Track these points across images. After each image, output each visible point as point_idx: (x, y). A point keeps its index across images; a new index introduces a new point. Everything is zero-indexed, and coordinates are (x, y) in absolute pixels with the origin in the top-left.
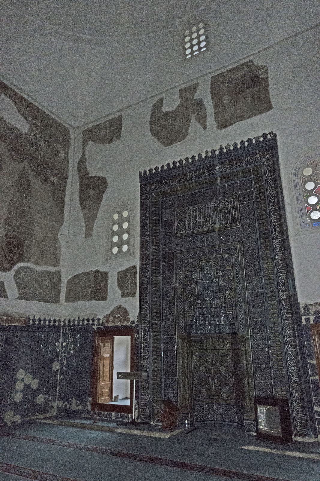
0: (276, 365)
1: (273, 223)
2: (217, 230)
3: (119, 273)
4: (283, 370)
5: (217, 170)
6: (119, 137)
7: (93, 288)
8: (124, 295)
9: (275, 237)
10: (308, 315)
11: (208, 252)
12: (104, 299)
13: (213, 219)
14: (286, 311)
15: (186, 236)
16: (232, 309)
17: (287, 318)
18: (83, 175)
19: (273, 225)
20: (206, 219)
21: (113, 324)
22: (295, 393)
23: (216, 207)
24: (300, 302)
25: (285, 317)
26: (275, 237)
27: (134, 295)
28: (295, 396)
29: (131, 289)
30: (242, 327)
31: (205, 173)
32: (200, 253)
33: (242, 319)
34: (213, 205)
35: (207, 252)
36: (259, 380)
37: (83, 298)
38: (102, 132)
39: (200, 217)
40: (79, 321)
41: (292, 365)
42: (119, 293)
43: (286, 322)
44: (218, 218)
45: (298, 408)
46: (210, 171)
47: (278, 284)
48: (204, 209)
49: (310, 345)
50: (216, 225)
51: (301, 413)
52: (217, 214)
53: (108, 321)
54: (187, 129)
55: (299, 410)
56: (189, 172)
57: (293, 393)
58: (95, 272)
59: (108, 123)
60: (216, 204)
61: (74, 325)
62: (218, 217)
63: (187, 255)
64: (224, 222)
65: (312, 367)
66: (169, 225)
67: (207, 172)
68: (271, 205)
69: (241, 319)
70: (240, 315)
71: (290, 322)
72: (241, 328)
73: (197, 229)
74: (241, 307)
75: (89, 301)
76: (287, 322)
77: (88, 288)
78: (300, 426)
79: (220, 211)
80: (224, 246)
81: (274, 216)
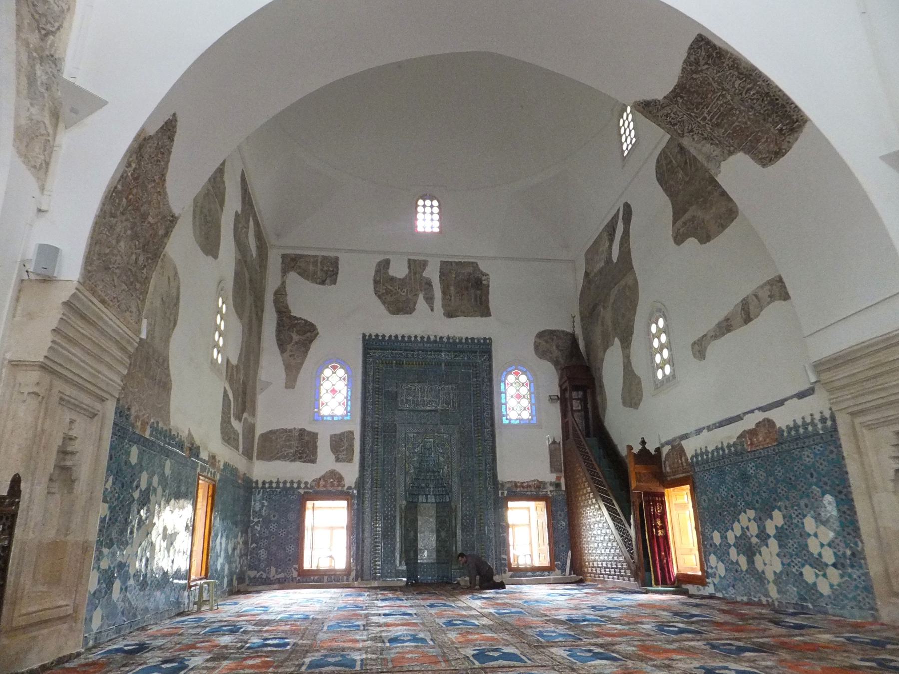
3: (331, 436)
6: (334, 282)
7: (297, 447)
8: (337, 460)
12: (313, 461)
15: (409, 411)
18: (283, 311)
20: (430, 398)
21: (324, 489)
27: (350, 460)
29: (346, 454)
37: (284, 458)
38: (311, 268)
40: (278, 482)
42: (333, 457)
47: (486, 465)
53: (318, 485)
54: (415, 303)
58: (301, 430)
59: (319, 260)
61: (270, 487)
66: (393, 397)
75: (291, 461)
77: (290, 447)
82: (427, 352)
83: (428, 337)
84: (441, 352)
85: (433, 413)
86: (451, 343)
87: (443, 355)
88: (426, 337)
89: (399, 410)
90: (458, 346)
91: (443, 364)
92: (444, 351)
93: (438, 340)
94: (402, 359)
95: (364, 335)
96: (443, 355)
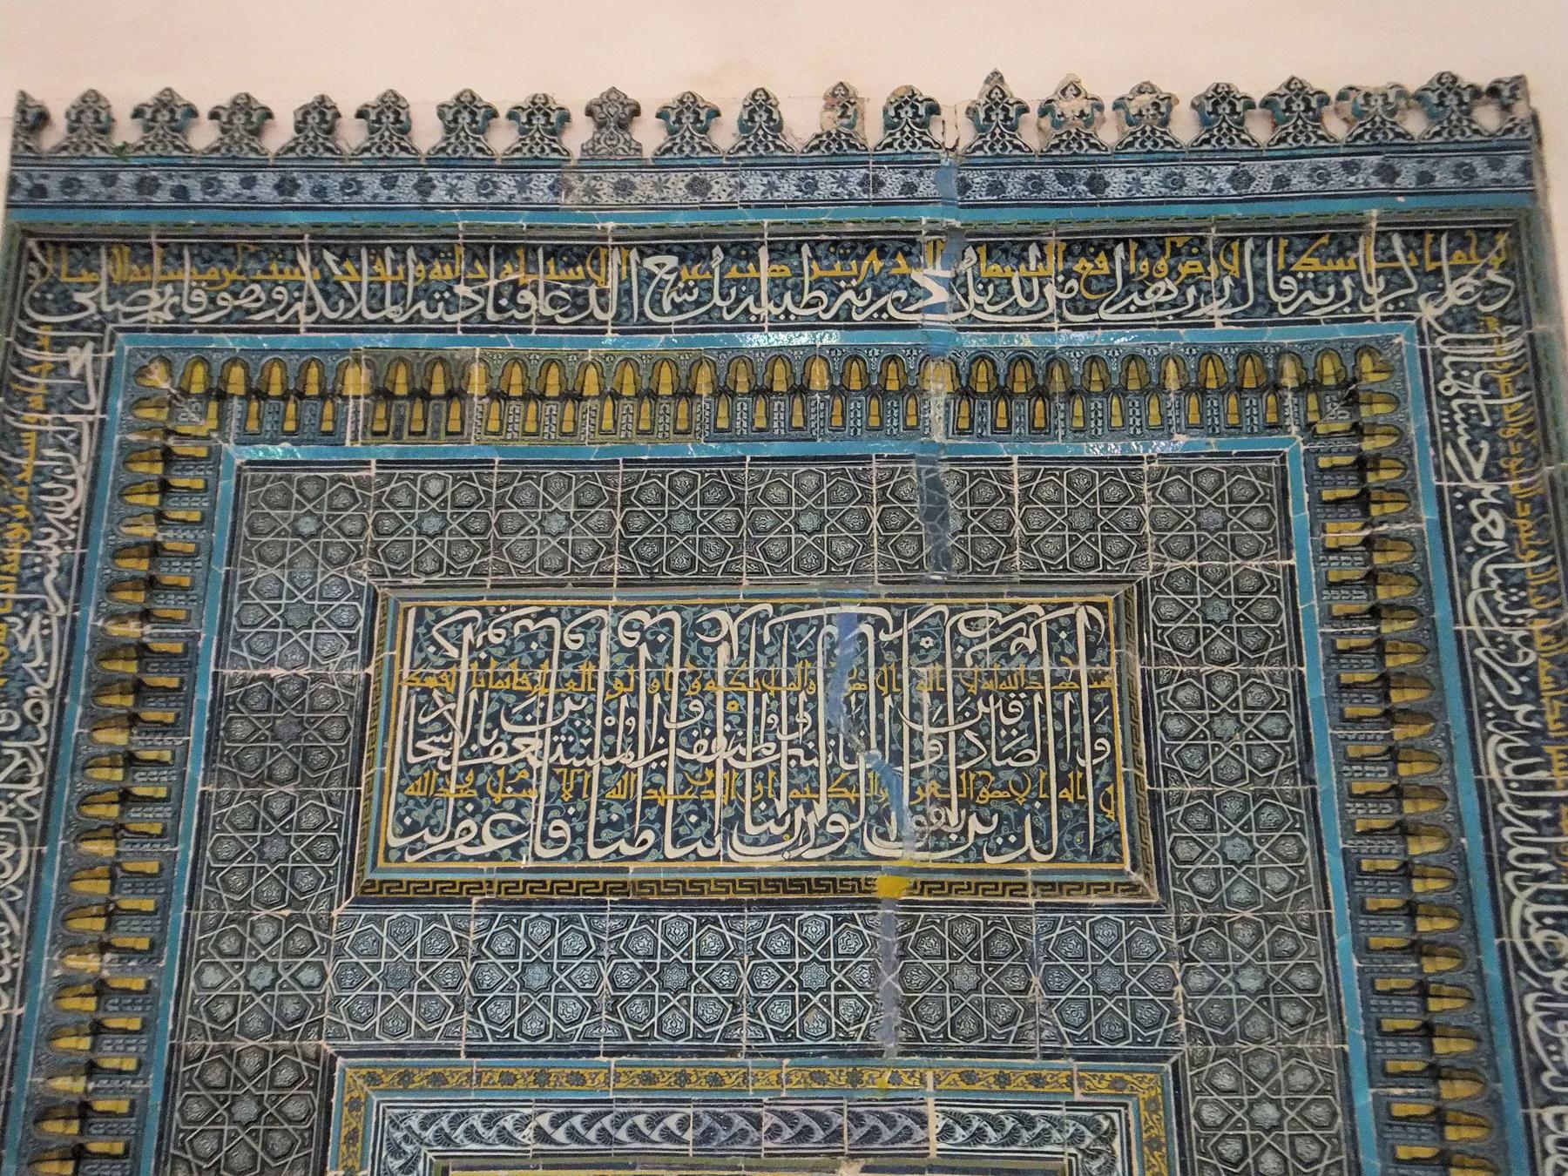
1: (1525, 934)
2: (886, 886)
5: (929, 294)
9: (1553, 1072)
11: (768, 1121)
13: (862, 765)
19: (1530, 946)
20: (781, 751)
23: (895, 647)
26: (1553, 1072)
31: (798, 290)
32: (671, 1122)
34: (867, 629)
35: (756, 1121)
39: (703, 724)
44: (915, 773)
46: (859, 291)
48: (761, 647)
50: (884, 836)
52: (896, 719)
56: (624, 241)
60: (898, 624)
62: (917, 754)
63: (508, 1123)
64: (975, 826)
67: (818, 283)
68: (1494, 748)
73: (658, 845)
79: (938, 696)
80: (968, 1077)
81: (1536, 858)
82: (743, 250)
83: (761, 110)
84: (908, 245)
85: (814, 923)
86: (1025, 159)
87: (931, 277)
88: (731, 117)
89: (378, 895)
90: (1117, 182)
91: (939, 384)
92: (950, 241)
93: (872, 132)
94: (462, 348)
95: (32, 119)
96: (931, 277)
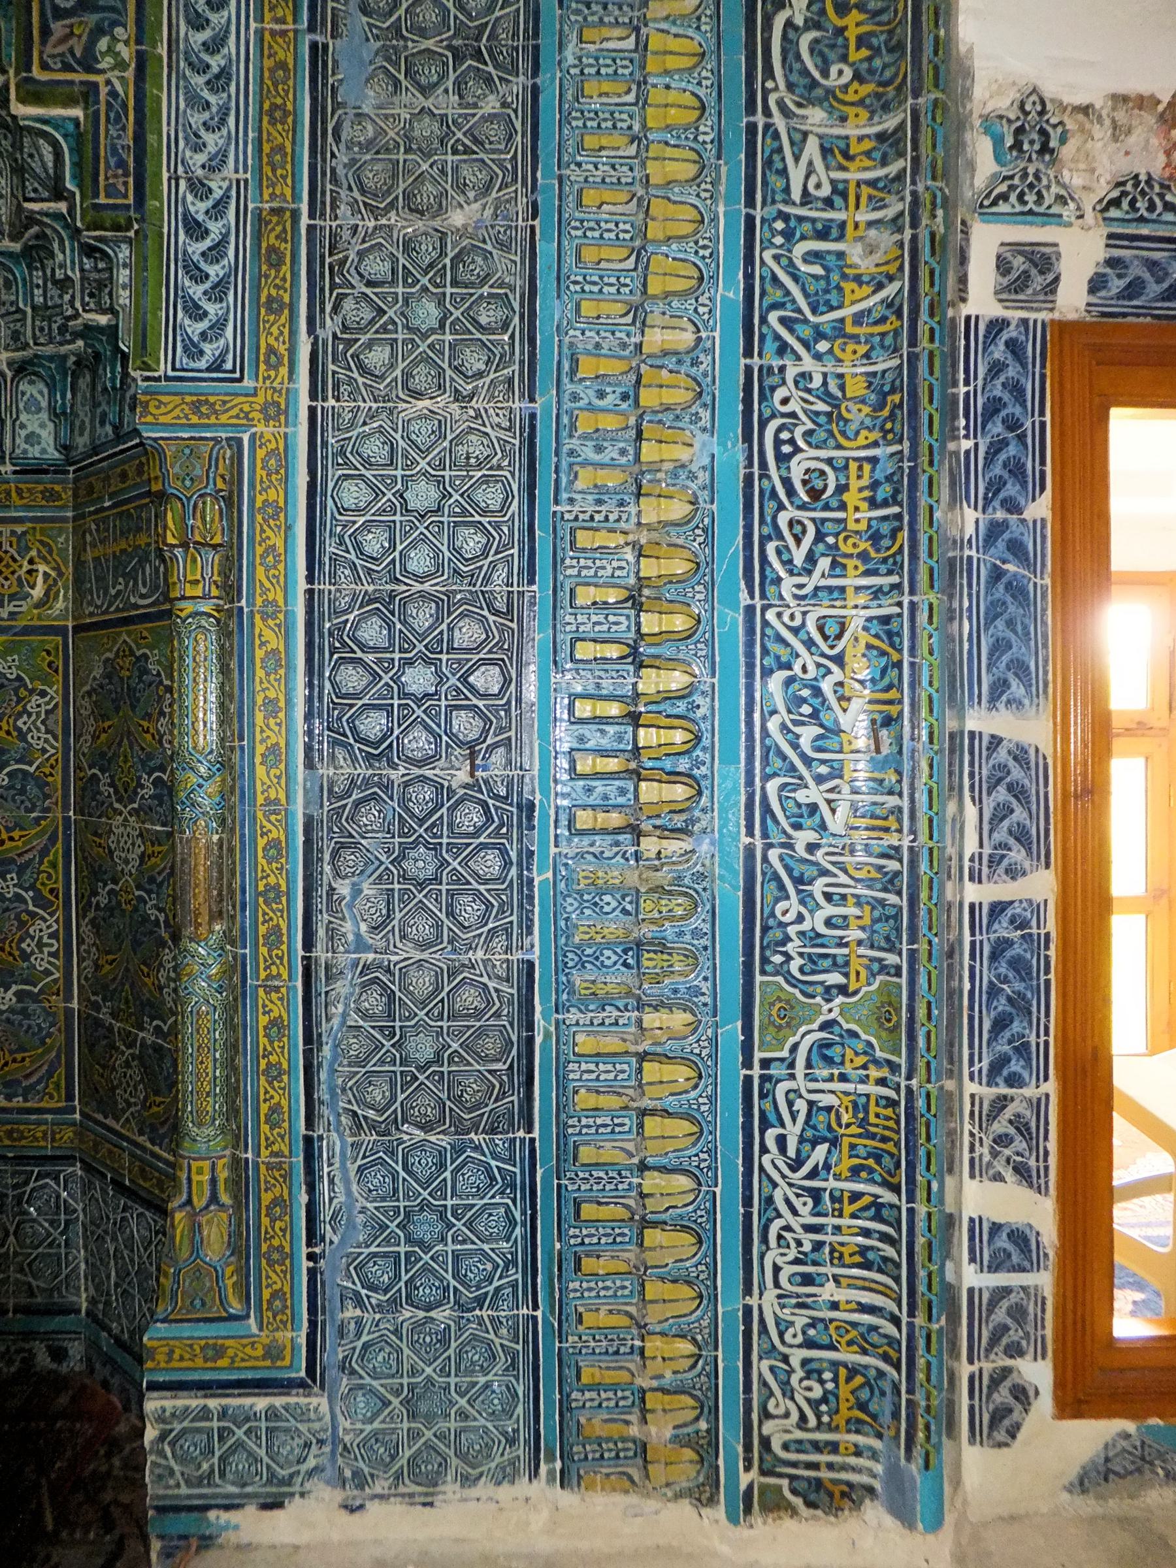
0: (613, 764)
4: (693, 821)
10: (1050, 218)
14: (816, 116)
16: (88, 63)
17: (829, 203)
22: (800, 1069)
24: (970, 50)
25: (796, 195)
28: (801, 1106)
30: (212, 308)
33: (218, 210)
36: (377, 940)
41: (807, 761)
43: (800, 249)
45: (809, 1228)
49: (1016, 549)
51: (836, 1279)
55: (817, 1246)
57: (775, 1071)
65: (998, 777)
69: (199, 208)
70: (198, 148)
71: (855, 253)
72: (196, 312)
74: (214, 46)
76: (814, 257)
78: (814, 1404)
